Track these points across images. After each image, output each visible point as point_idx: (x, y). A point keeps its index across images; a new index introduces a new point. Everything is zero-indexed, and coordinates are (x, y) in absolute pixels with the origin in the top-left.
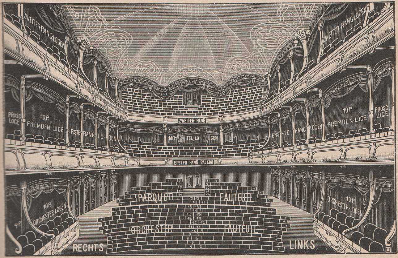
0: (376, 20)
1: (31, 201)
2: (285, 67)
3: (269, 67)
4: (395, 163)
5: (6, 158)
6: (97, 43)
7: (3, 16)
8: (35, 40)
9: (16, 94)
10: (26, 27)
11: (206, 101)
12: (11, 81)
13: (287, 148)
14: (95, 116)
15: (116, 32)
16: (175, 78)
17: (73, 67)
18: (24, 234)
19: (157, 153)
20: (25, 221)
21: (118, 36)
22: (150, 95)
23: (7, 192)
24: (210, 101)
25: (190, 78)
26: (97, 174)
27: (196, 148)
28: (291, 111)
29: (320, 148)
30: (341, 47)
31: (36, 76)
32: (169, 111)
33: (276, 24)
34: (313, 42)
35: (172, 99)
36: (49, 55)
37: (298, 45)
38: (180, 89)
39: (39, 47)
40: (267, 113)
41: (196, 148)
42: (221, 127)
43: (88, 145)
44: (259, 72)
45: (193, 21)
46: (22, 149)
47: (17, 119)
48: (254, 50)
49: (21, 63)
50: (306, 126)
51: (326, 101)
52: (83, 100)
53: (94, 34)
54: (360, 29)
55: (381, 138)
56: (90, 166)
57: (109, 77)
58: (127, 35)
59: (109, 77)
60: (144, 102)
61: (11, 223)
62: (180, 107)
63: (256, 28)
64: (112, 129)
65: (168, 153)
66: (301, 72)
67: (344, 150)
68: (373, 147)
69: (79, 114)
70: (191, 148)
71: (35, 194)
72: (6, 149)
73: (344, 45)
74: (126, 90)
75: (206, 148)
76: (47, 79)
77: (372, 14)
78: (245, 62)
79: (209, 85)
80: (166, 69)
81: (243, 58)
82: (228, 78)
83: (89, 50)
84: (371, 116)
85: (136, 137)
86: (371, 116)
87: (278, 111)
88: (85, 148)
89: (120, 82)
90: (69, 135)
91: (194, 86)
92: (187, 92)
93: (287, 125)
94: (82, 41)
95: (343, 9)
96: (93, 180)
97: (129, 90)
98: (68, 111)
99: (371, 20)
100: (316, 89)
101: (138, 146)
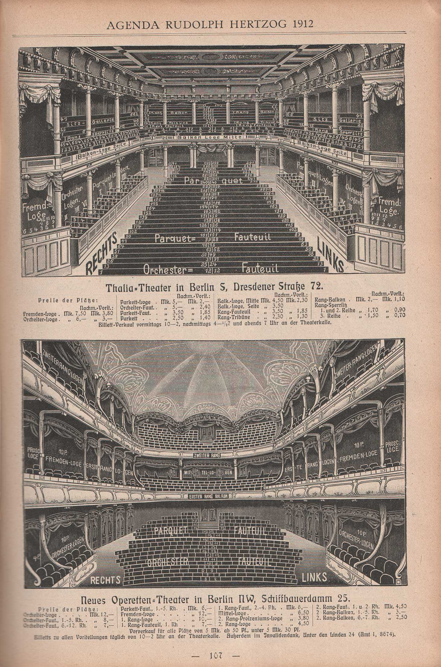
0: (386, 356)
1: (49, 534)
2: (298, 403)
3: (282, 403)
4: (406, 497)
5: (25, 492)
6: (114, 379)
7: (22, 353)
8: (54, 376)
9: (35, 429)
10: (44, 364)
11: (220, 436)
12: (30, 416)
13: (300, 483)
14: (112, 451)
15: (133, 368)
16: (190, 414)
17: (91, 402)
18: (43, 566)
19: (172, 487)
20: (44, 554)
21: (135, 372)
22: (166, 430)
23: (26, 525)
24: (225, 436)
25: (205, 413)
26: (114, 507)
27: (211, 483)
28: (304, 446)
29: (332, 482)
30: (353, 383)
31: (54, 412)
32: (184, 446)
33: (289, 361)
34: (325, 378)
35: (187, 434)
36: (67, 391)
37: (310, 381)
38: (195, 424)
39: (58, 383)
40: (280, 448)
41: (211, 483)
42: (235, 461)
43: (105, 479)
44: (272, 408)
45: (208, 357)
46: (40, 483)
47: (36, 454)
48: (267, 386)
49: (39, 399)
50: (318, 460)
51: (337, 437)
52: (101, 435)
53: (111, 371)
54: (371, 366)
55: (392, 473)
56: (107, 500)
57: (126, 412)
58: (143, 371)
59: (126, 412)
60: (160, 437)
61: (30, 556)
62: (195, 442)
63: (269, 365)
64: (129, 464)
65: (183, 487)
66: (313, 408)
67: (355, 484)
68: (384, 481)
69: (96, 449)
70: (206, 483)
71: (54, 527)
72: (25, 483)
73: (355, 381)
74: (143, 425)
75: (221, 482)
76: (65, 415)
77: (383, 351)
78: (259, 398)
79: (223, 421)
80: (182, 405)
81: (257, 394)
82: (242, 414)
83: (107, 386)
84: (382, 451)
85: (153, 471)
86: (382, 451)
87: (291, 446)
88: (102, 482)
89: (136, 417)
90: (87, 469)
91: (209, 421)
92: (202, 428)
93: (300, 460)
94: (99, 377)
95: (354, 345)
96: (110, 514)
97: (146, 425)
98: (86, 446)
99: (382, 357)
100: (328, 425)
101: (154, 481)
